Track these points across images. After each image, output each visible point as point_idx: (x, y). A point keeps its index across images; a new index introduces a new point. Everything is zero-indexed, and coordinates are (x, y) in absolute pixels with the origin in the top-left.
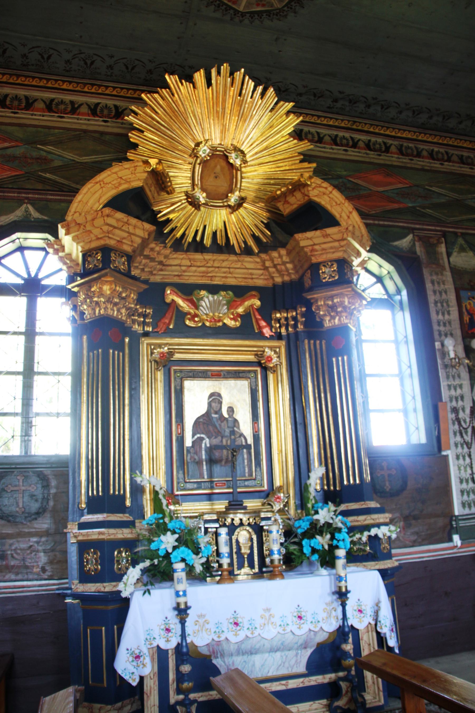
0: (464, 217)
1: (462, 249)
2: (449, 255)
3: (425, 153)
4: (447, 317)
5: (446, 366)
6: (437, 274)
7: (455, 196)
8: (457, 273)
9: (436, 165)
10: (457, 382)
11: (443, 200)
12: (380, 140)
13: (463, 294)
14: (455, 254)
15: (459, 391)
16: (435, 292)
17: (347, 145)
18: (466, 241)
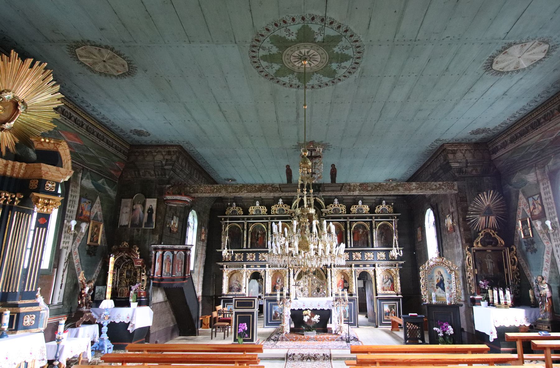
0: (94, 164)
1: (88, 178)
2: (82, 179)
3: (95, 133)
4: (72, 209)
5: (65, 232)
6: (75, 187)
7: (97, 155)
8: (83, 188)
9: (98, 140)
10: (68, 240)
11: (91, 154)
12: (81, 120)
13: (83, 199)
14: (84, 179)
15: (67, 245)
16: (71, 195)
17: (67, 117)
18: (91, 175)
